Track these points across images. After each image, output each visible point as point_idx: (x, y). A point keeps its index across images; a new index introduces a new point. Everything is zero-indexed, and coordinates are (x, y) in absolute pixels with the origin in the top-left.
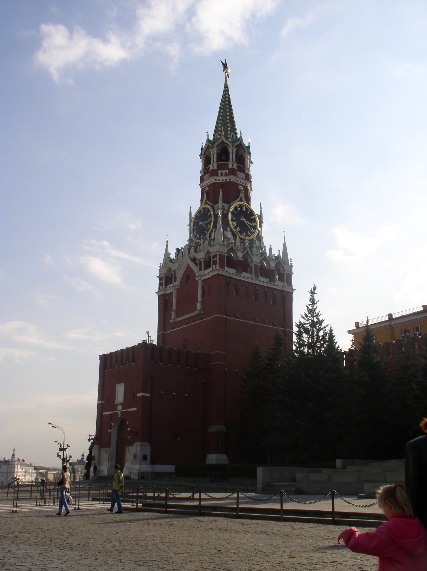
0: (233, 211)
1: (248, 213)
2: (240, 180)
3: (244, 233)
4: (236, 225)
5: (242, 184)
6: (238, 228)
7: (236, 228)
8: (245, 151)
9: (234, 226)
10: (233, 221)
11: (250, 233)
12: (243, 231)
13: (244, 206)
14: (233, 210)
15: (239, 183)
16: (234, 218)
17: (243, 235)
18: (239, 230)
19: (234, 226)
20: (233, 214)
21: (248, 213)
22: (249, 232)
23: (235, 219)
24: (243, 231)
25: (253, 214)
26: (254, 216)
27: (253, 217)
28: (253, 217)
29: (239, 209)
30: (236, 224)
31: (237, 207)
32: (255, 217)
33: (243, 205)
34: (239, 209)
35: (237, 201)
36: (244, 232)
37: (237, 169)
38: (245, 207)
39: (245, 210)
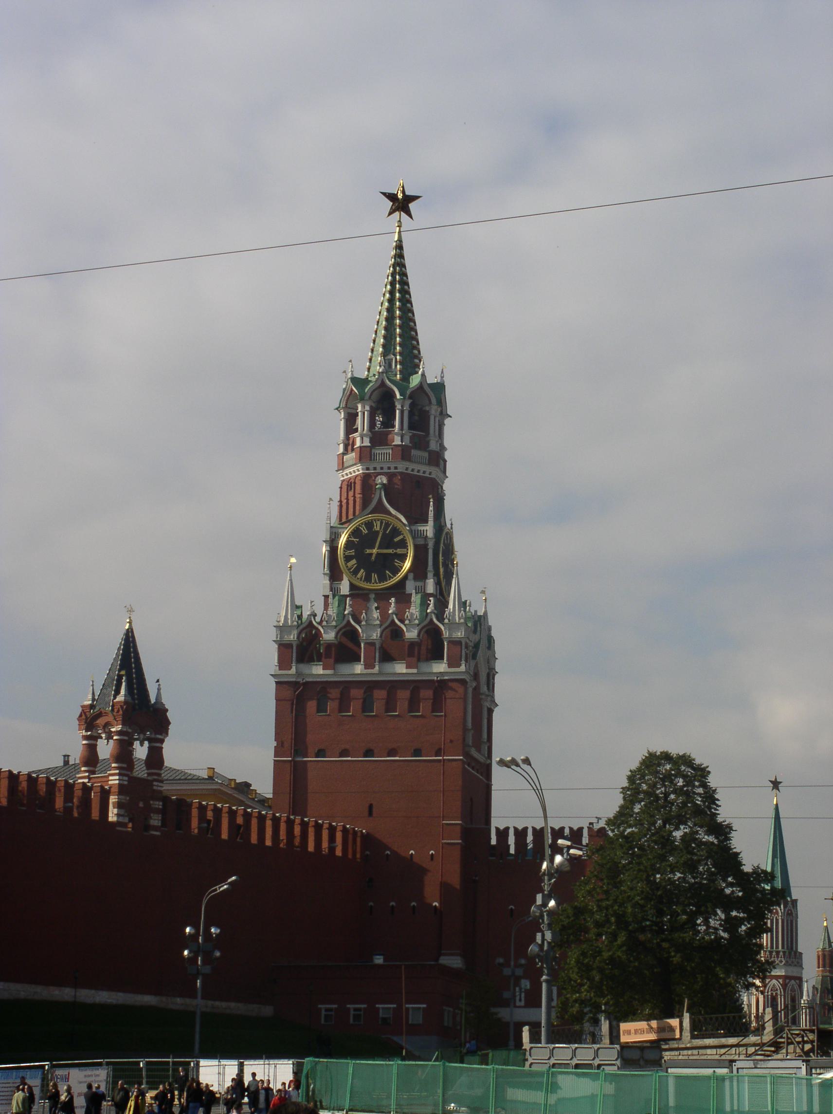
0: (350, 539)
3: (374, 576)
4: (355, 566)
5: (386, 470)
6: (362, 570)
7: (355, 572)
9: (351, 570)
10: (348, 559)
11: (389, 574)
12: (373, 574)
13: (378, 521)
14: (351, 538)
15: (379, 471)
16: (352, 552)
17: (373, 581)
18: (364, 573)
19: (351, 570)
21: (387, 532)
23: (353, 554)
24: (373, 574)
27: (401, 537)
28: (401, 537)
29: (365, 531)
30: (355, 564)
31: (360, 527)
33: (375, 520)
34: (365, 531)
35: (366, 514)
36: (376, 576)
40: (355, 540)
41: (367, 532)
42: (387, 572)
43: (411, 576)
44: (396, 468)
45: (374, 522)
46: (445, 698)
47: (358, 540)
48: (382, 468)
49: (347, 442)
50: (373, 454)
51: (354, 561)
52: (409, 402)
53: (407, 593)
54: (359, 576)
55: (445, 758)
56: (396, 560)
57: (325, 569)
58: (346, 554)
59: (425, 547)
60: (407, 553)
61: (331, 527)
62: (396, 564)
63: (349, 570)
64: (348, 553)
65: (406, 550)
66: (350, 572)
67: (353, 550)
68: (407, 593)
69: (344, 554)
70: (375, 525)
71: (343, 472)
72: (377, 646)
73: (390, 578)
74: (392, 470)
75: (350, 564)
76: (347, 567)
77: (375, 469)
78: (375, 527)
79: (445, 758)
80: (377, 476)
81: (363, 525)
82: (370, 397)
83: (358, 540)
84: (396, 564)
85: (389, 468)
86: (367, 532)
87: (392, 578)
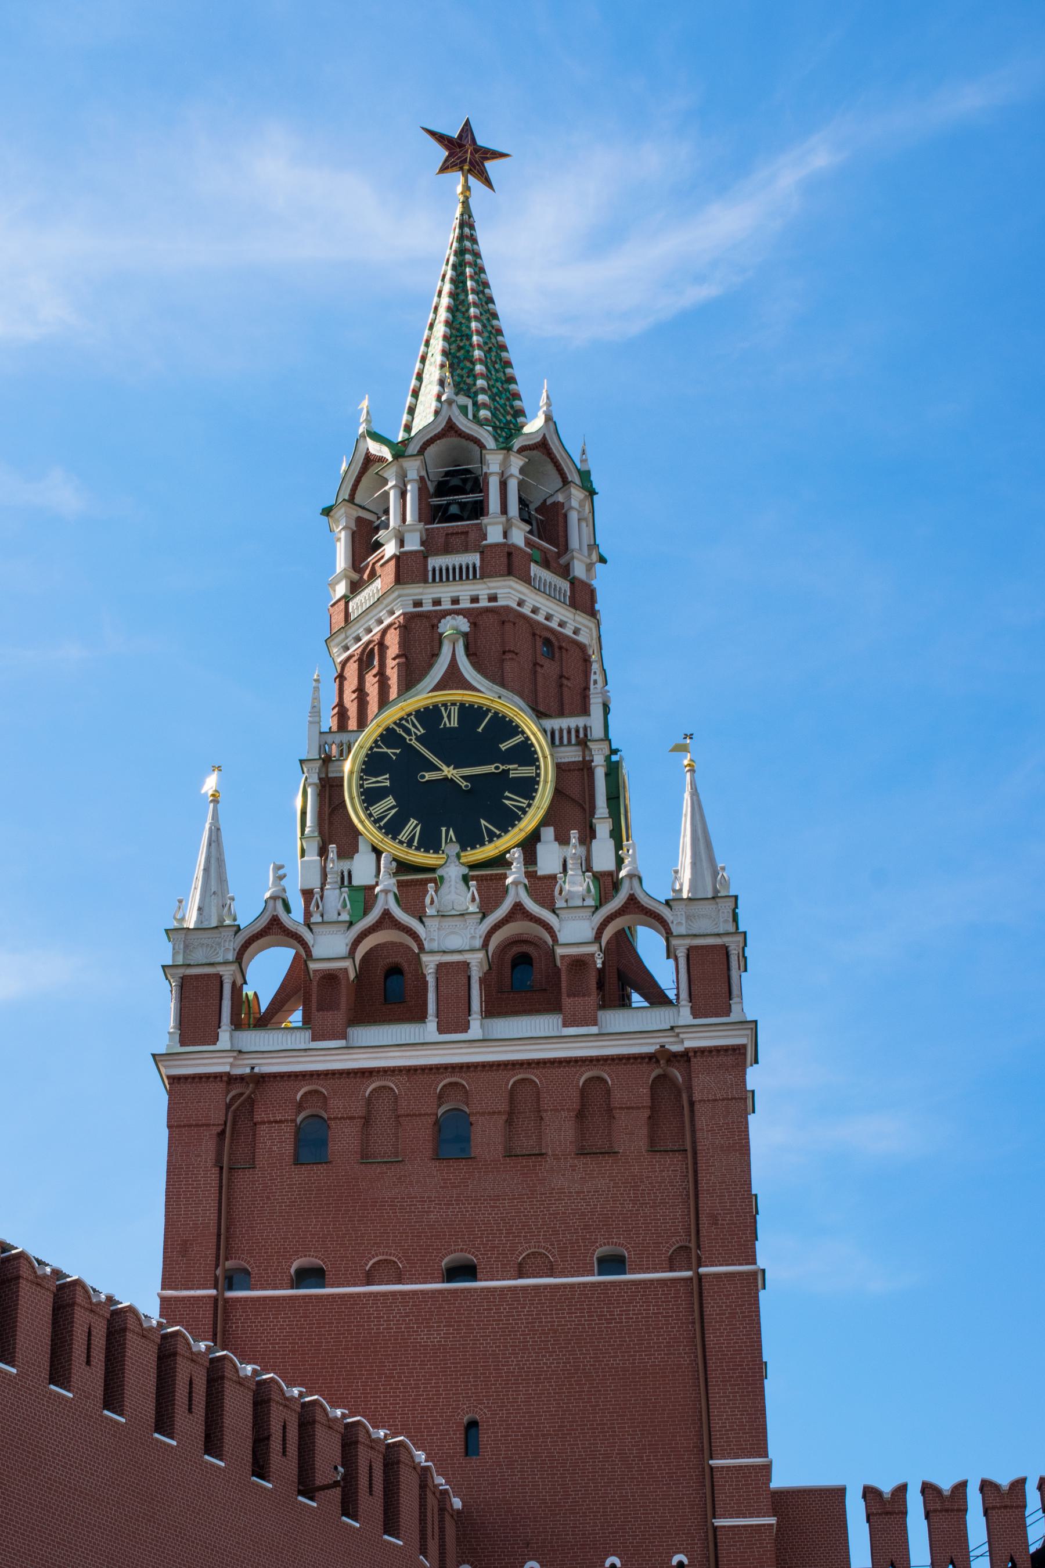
0: (375, 750)
1: (480, 730)
2: (446, 592)
4: (394, 811)
5: (465, 604)
6: (413, 822)
8: (482, 446)
9: (382, 824)
10: (370, 797)
12: (444, 829)
14: (379, 747)
15: (446, 605)
16: (384, 781)
19: (382, 824)
20: (373, 764)
21: (480, 730)
22: (483, 822)
23: (388, 784)
24: (444, 829)
25: (517, 726)
26: (523, 732)
32: (528, 738)
33: (443, 705)
36: (451, 833)
37: (422, 548)
38: (455, 711)
39: (454, 723)
40: (385, 750)
41: (423, 731)
42: (483, 822)
43: (548, 833)
44: (493, 598)
45: (443, 709)
46: (692, 1104)
47: (398, 751)
48: (455, 601)
49: (355, 577)
50: (430, 568)
51: (390, 801)
52: (521, 463)
53: (539, 873)
54: (404, 836)
55: (702, 1270)
56: (507, 794)
57: (307, 830)
58: (365, 786)
59: (586, 768)
60: (538, 775)
61: (321, 733)
62: (507, 802)
63: (375, 822)
64: (371, 782)
65: (534, 768)
66: (380, 828)
67: (387, 776)
68: (539, 873)
69: (362, 786)
70: (445, 715)
71: (347, 637)
72: (476, 974)
73: (492, 837)
74: (484, 603)
75: (377, 809)
76: (370, 815)
77: (437, 602)
78: (446, 719)
79: (702, 1270)
80: (444, 617)
81: (412, 717)
82: (422, 451)
83: (398, 751)
84: (507, 802)
85: (475, 599)
86: (423, 731)
87: (499, 837)
